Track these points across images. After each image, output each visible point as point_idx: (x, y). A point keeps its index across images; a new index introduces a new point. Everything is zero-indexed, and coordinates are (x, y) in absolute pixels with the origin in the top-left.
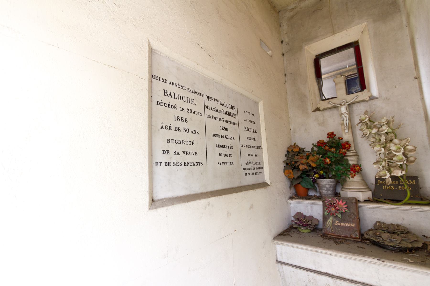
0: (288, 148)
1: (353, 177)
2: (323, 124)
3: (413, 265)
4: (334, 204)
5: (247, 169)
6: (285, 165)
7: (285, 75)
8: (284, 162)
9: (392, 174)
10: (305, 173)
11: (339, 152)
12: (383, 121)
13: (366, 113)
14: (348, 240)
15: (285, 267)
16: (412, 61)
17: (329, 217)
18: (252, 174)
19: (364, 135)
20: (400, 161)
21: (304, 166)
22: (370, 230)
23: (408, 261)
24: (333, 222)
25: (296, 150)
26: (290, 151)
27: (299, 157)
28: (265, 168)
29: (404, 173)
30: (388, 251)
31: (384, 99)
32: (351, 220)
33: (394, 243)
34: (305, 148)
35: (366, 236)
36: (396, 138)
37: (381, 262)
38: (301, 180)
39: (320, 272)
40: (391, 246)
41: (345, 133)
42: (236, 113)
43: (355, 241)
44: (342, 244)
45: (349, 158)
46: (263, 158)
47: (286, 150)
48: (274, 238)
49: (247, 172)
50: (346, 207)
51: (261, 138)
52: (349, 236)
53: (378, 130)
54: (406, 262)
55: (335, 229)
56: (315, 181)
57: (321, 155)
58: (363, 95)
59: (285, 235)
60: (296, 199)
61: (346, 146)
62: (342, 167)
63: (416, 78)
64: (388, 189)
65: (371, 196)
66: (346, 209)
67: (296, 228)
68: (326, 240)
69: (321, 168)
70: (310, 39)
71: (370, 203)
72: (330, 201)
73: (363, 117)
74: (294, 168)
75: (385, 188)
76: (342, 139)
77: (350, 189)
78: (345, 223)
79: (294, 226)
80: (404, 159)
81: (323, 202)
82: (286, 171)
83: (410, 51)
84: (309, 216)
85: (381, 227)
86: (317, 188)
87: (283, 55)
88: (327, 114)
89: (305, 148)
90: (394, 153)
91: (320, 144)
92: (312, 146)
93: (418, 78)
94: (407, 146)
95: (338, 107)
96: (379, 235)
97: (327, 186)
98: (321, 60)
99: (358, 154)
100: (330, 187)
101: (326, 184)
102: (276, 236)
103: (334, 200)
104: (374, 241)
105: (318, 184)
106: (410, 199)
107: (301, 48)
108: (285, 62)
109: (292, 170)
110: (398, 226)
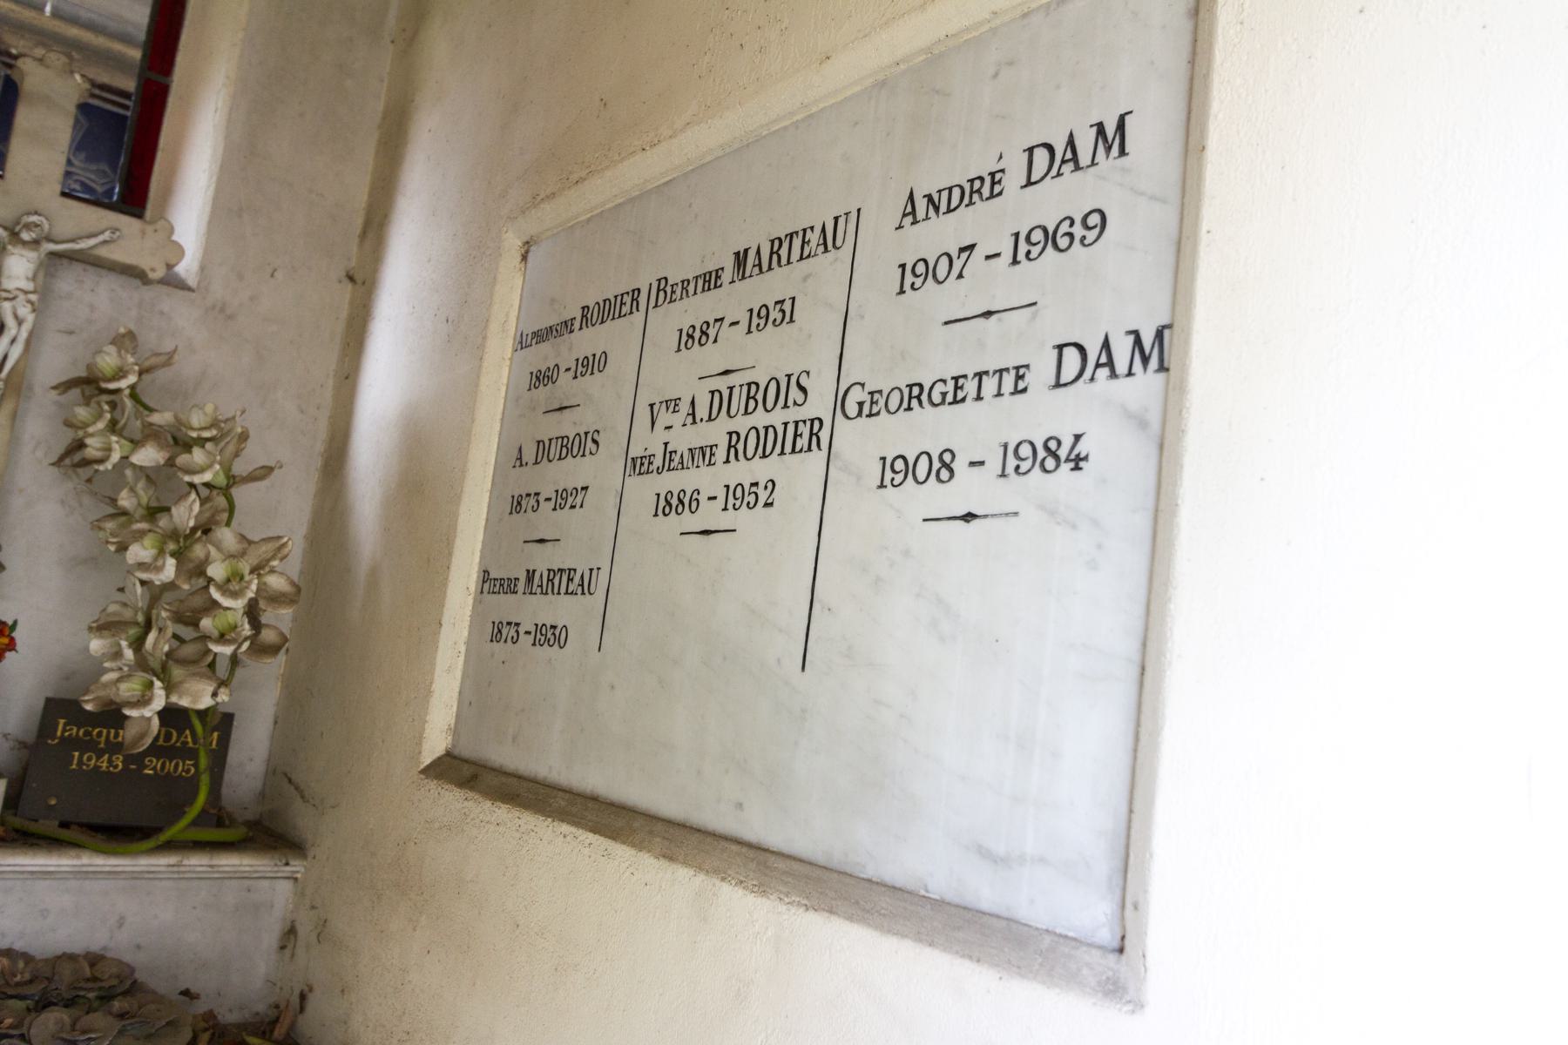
9: (174, 699)
12: (196, 419)
16: (361, 197)
20: (222, 638)
31: (214, 307)
36: (228, 524)
53: (170, 462)
58: (125, 238)
63: (351, 278)
64: (97, 768)
73: (108, 360)
75: (80, 762)
80: (247, 630)
90: (215, 594)
93: (362, 283)
94: (272, 571)
106: (195, 823)
110: (94, 959)
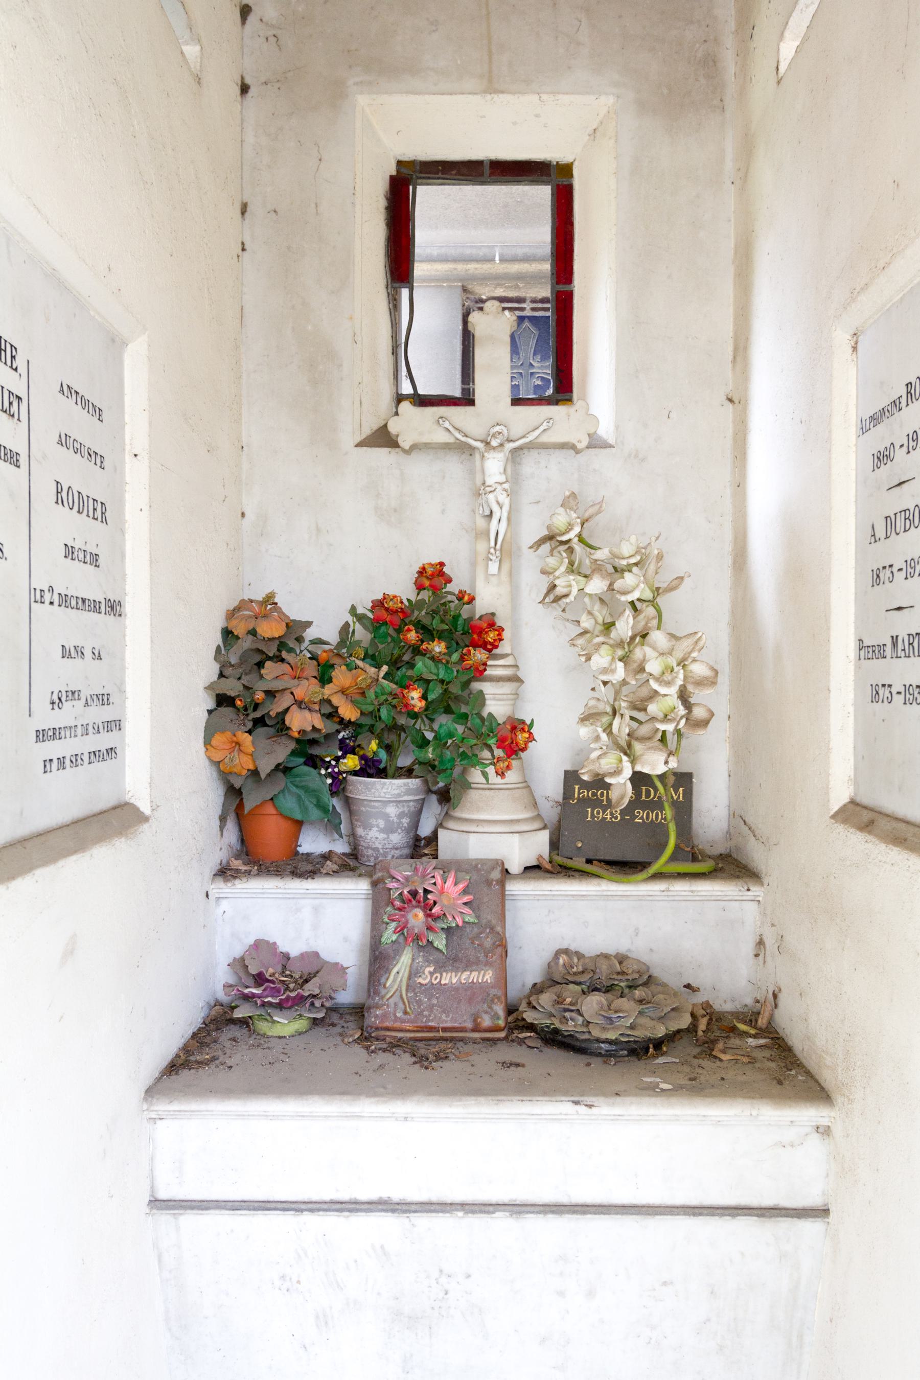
0: (232, 614)
1: (502, 775)
2: (394, 514)
3: (673, 1100)
4: (426, 891)
5: (55, 734)
6: (211, 704)
7: (244, 209)
8: (209, 688)
9: (638, 768)
10: (308, 750)
11: (462, 658)
12: (626, 549)
13: (570, 501)
14: (461, 1040)
15: (189, 1219)
16: (728, 329)
17: (398, 953)
18: (76, 760)
19: (553, 597)
20: (666, 719)
21: (306, 713)
22: (537, 989)
23: (657, 1085)
24: (414, 973)
25: (270, 629)
26: (240, 629)
27: (285, 667)
28: (129, 726)
29: (673, 764)
30: (596, 1062)
31: (630, 455)
32: (482, 956)
33: (617, 1028)
34: (309, 624)
35: (530, 1016)
36: (659, 628)
37: (582, 1109)
38: (282, 781)
39: (356, 1202)
40: (607, 1041)
41: (488, 576)
42: (23, 394)
43: (484, 1039)
44: (446, 1064)
45: (487, 688)
46: (123, 669)
47: (219, 623)
48: (151, 1092)
49: (54, 749)
50: (465, 904)
51: (123, 556)
52: (469, 1025)
53: (611, 588)
54: (652, 1090)
55: (419, 1003)
56: (338, 786)
57: (385, 668)
58: (559, 421)
59: (200, 1064)
60: (248, 873)
61: (481, 635)
62: (460, 729)
63: (730, 400)
64: (604, 819)
65: (545, 850)
66: (466, 910)
67: (245, 1023)
68: (381, 1058)
69: (379, 726)
70: (389, 68)
71: (544, 878)
72: (407, 879)
73: (561, 520)
74: (260, 722)
75: (593, 816)
76: (472, 600)
77: (466, 820)
78: (456, 970)
79: (238, 1014)
80: (682, 711)
81: (374, 884)
82: (217, 740)
83: (727, 290)
84: (303, 956)
85: (576, 974)
86: (344, 816)
87: (245, 89)
88: (420, 468)
89: (309, 624)
90: (654, 685)
91: (386, 616)
92: (350, 619)
93: (737, 401)
94: (694, 660)
95: (472, 449)
96: (571, 1004)
97: (392, 811)
98: (420, 189)
99: (520, 674)
100: (401, 815)
101: (386, 802)
102: (159, 1080)
103: (424, 876)
104: (556, 1031)
105: (348, 802)
106: (674, 858)
107: (336, 95)
108: (250, 139)
109: (250, 732)
110: (622, 959)
